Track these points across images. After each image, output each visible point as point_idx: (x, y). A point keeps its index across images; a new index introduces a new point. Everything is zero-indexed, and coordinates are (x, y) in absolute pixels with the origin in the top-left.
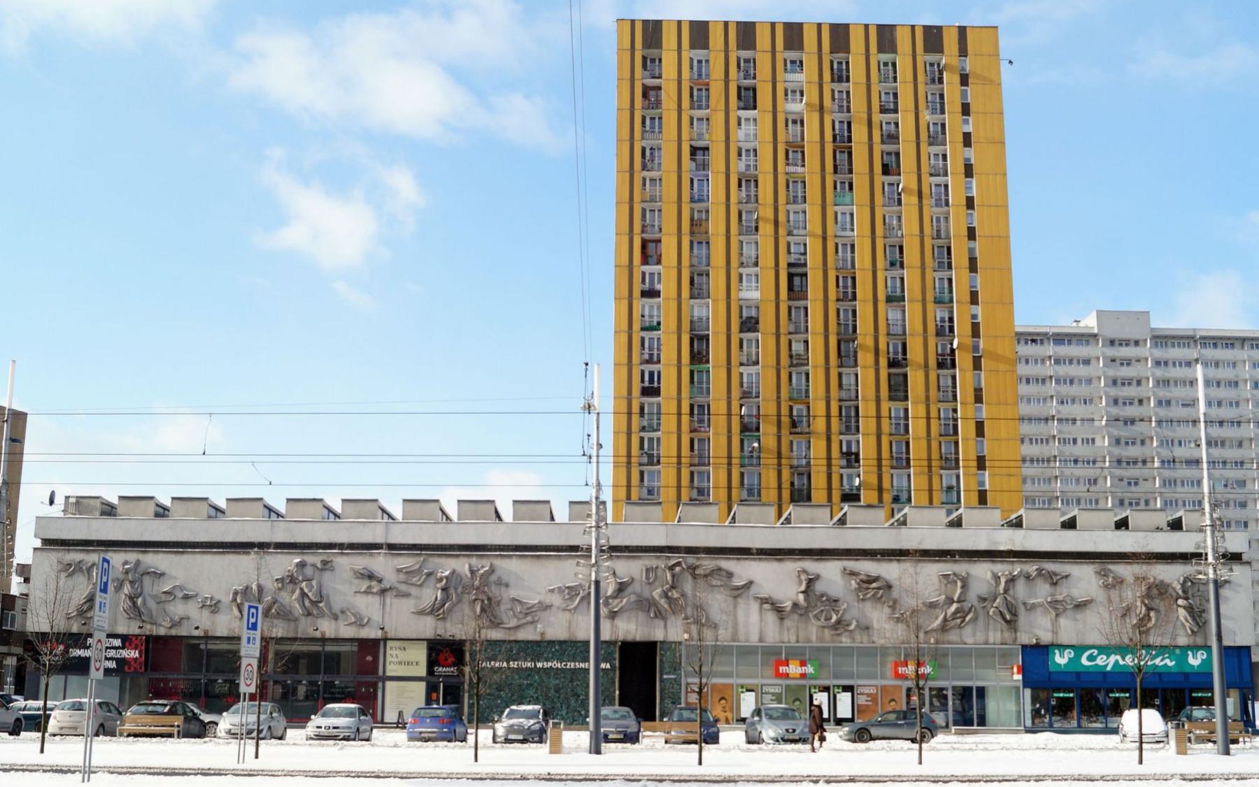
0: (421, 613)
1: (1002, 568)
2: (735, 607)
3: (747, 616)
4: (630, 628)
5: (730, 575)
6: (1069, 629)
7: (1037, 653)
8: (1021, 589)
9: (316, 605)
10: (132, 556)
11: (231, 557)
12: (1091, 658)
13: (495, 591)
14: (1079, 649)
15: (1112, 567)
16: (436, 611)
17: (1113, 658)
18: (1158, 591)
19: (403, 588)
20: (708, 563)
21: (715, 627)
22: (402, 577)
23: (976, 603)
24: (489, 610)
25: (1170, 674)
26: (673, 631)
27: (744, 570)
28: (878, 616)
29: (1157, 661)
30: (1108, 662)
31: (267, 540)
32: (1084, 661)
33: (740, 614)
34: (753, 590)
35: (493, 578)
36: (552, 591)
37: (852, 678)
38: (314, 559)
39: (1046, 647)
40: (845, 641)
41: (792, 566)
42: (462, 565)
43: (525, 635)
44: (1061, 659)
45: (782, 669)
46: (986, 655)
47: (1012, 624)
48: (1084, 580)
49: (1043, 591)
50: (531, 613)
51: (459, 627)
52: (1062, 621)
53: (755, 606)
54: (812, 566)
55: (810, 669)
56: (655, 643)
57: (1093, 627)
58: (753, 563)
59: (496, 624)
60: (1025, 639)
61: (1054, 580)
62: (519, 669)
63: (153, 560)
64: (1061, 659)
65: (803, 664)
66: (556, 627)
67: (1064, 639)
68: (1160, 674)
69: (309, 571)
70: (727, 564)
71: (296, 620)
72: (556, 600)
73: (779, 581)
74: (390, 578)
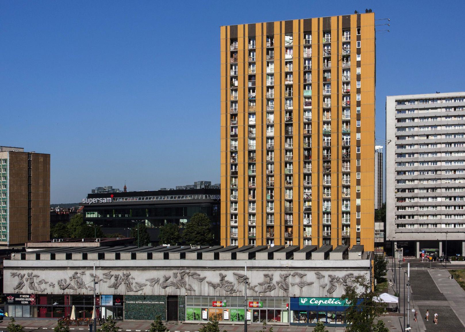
0: (110, 287)
1: (284, 273)
2: (201, 285)
3: (204, 288)
4: (170, 291)
5: (199, 275)
6: (306, 291)
7: (295, 300)
8: (290, 280)
9: (81, 285)
10: (30, 271)
11: (58, 271)
12: (313, 301)
13: (131, 280)
14: (309, 298)
15: (321, 272)
16: (115, 286)
17: (320, 301)
18: (333, 279)
19: (105, 280)
20: (192, 271)
21: (195, 291)
22: (105, 276)
23: (276, 284)
24: (129, 286)
25: (340, 307)
26: (182, 292)
27: (203, 274)
28: (242, 287)
29: (336, 303)
30: (319, 302)
31: (66, 266)
32: (311, 302)
33: (202, 287)
34: (207, 280)
35: (130, 277)
36: (147, 280)
37: (273, 307)
38: (79, 271)
39: (298, 298)
40: (234, 295)
41: (218, 272)
42: (120, 273)
43: (139, 293)
44: (303, 302)
45: (215, 304)
46: (278, 299)
47: (286, 290)
48: (311, 276)
49: (297, 280)
50: (141, 286)
51: (122, 290)
52: (304, 289)
53: (207, 285)
54: (224, 272)
55: (260, 305)
56: (122, 296)
57: (315, 291)
58: (206, 272)
59: (132, 290)
60: (291, 295)
61: (302, 276)
62: (138, 304)
63: (35, 272)
64: (303, 302)
65: (258, 303)
66: (147, 291)
67: (304, 295)
68: (336, 307)
69: (79, 275)
70: (199, 272)
71: (76, 290)
72: (148, 283)
73: (213, 277)
74: (101, 277)
